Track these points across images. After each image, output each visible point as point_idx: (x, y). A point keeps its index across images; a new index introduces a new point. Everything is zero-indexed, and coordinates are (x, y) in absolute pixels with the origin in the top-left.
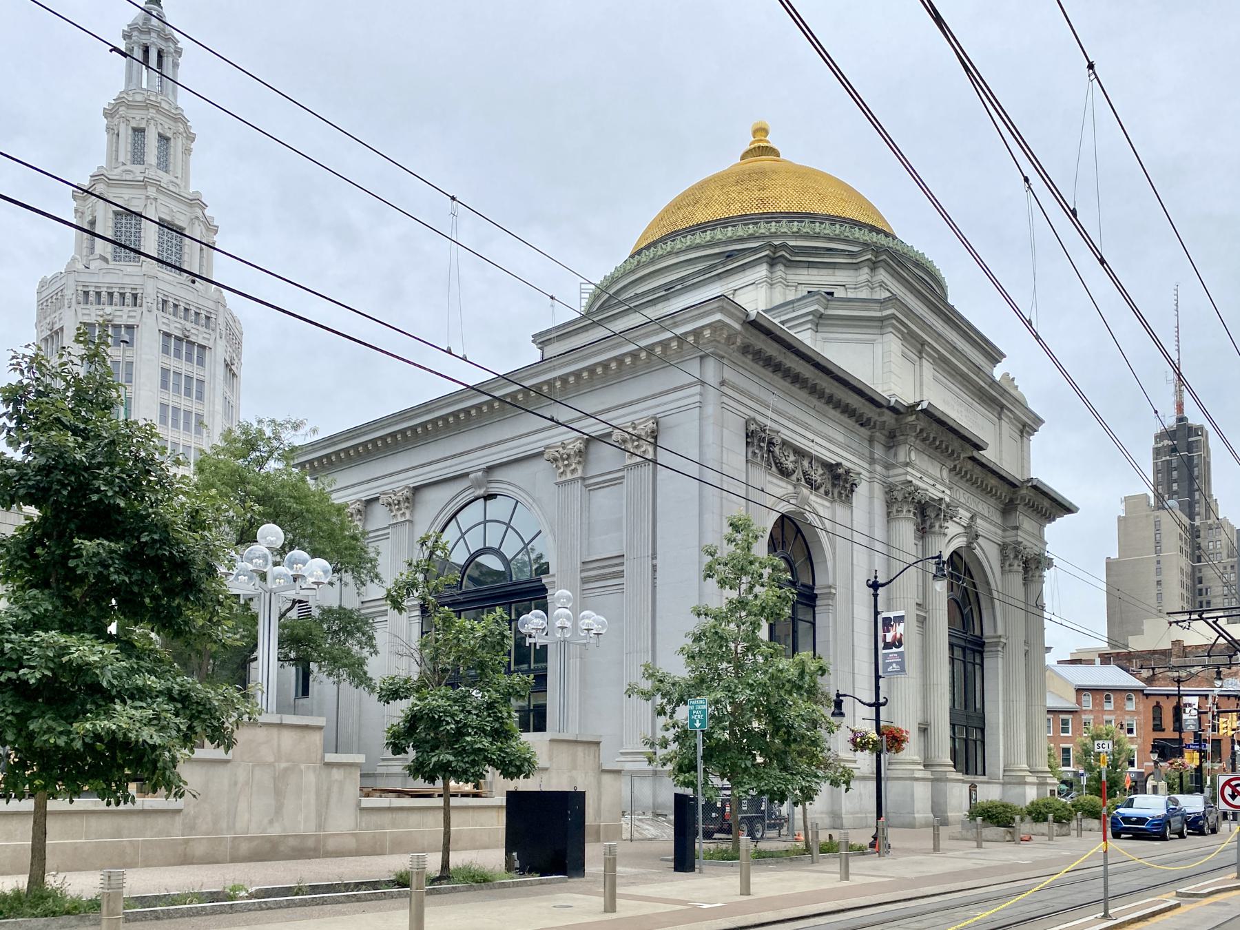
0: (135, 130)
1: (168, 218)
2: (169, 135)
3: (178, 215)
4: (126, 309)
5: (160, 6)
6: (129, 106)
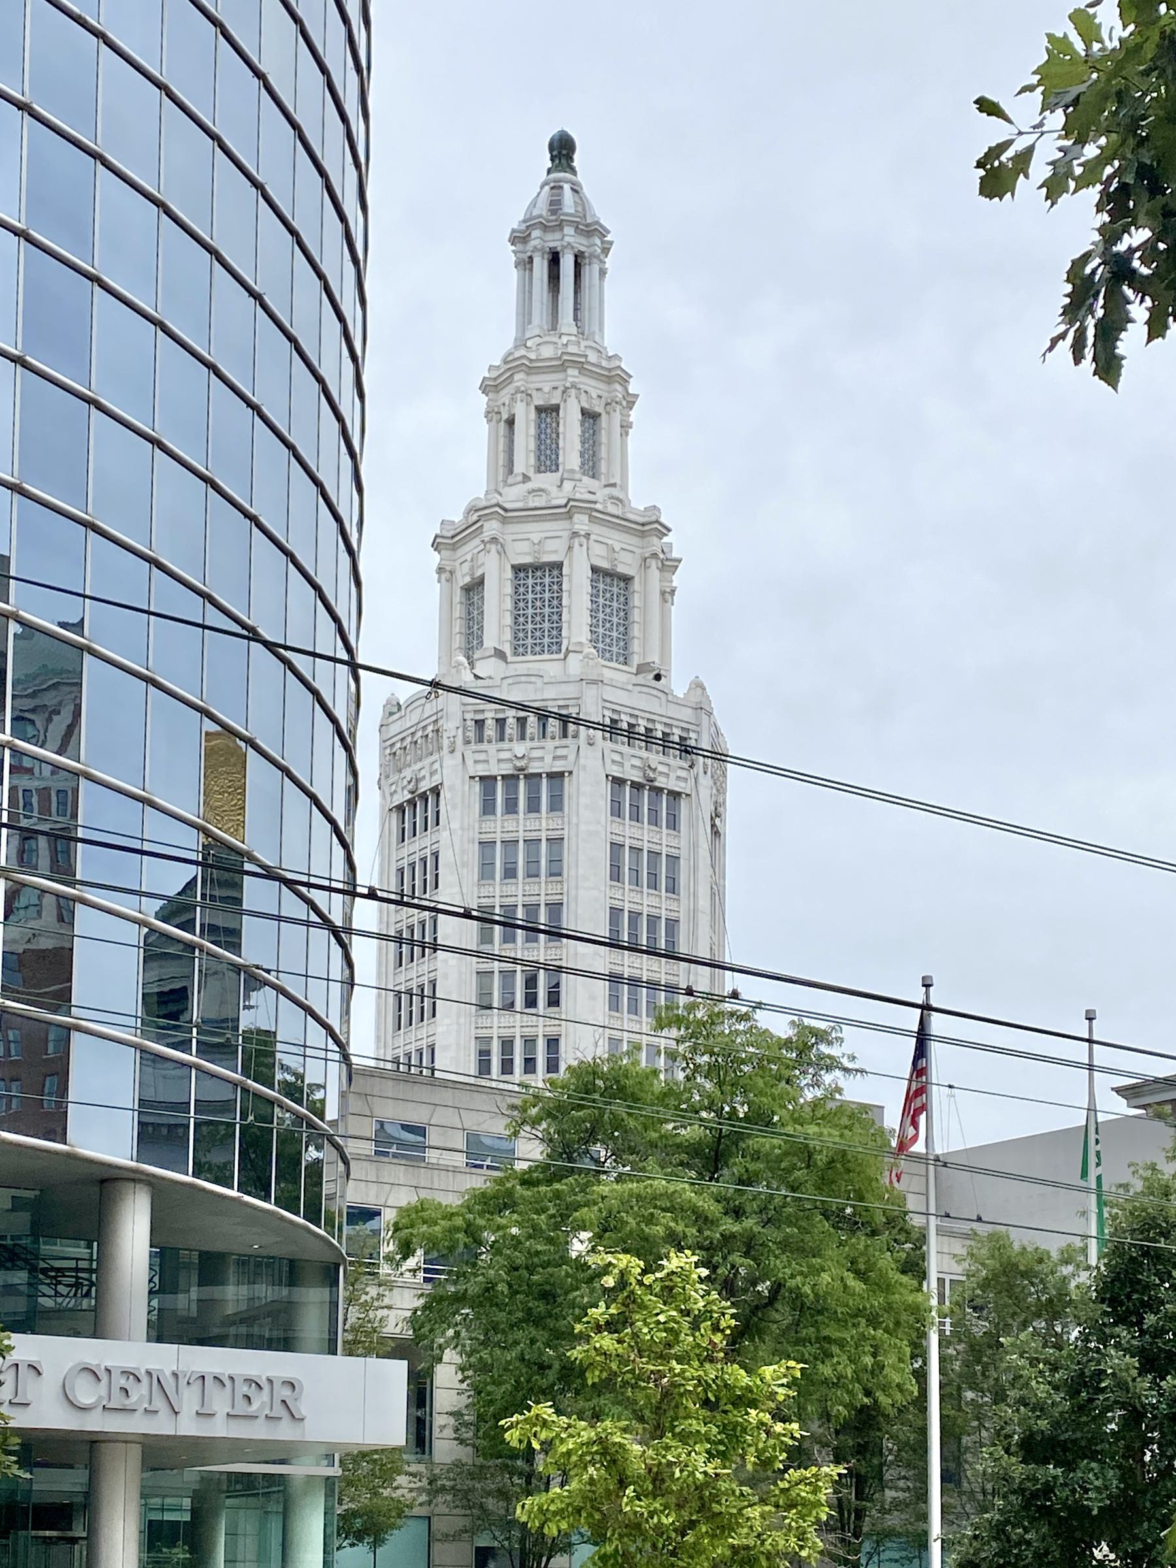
0: (540, 410)
1: (605, 564)
4: (549, 744)
5: (573, 171)
6: (531, 369)
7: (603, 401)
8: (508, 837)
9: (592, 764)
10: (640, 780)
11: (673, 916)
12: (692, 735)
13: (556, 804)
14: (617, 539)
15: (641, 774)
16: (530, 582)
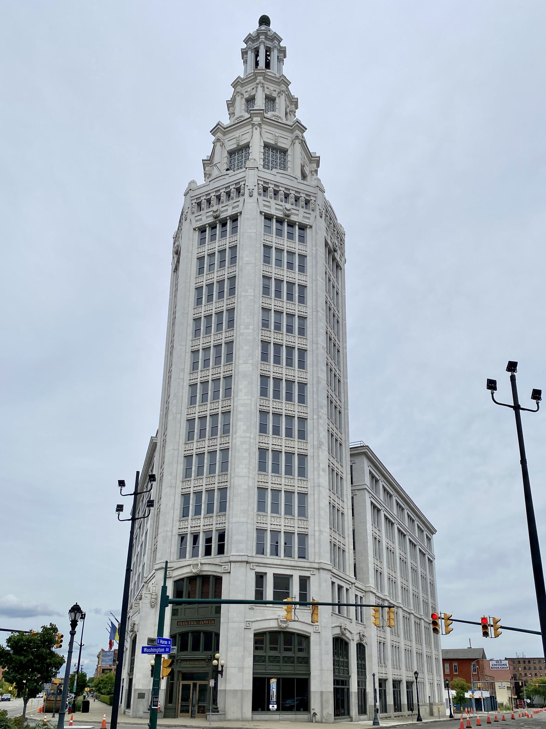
1: (272, 142)
2: (275, 95)
6: (243, 85)
7: (277, 92)
8: (210, 252)
10: (282, 216)
12: (312, 198)
13: (235, 230)
14: (278, 132)
15: (282, 213)
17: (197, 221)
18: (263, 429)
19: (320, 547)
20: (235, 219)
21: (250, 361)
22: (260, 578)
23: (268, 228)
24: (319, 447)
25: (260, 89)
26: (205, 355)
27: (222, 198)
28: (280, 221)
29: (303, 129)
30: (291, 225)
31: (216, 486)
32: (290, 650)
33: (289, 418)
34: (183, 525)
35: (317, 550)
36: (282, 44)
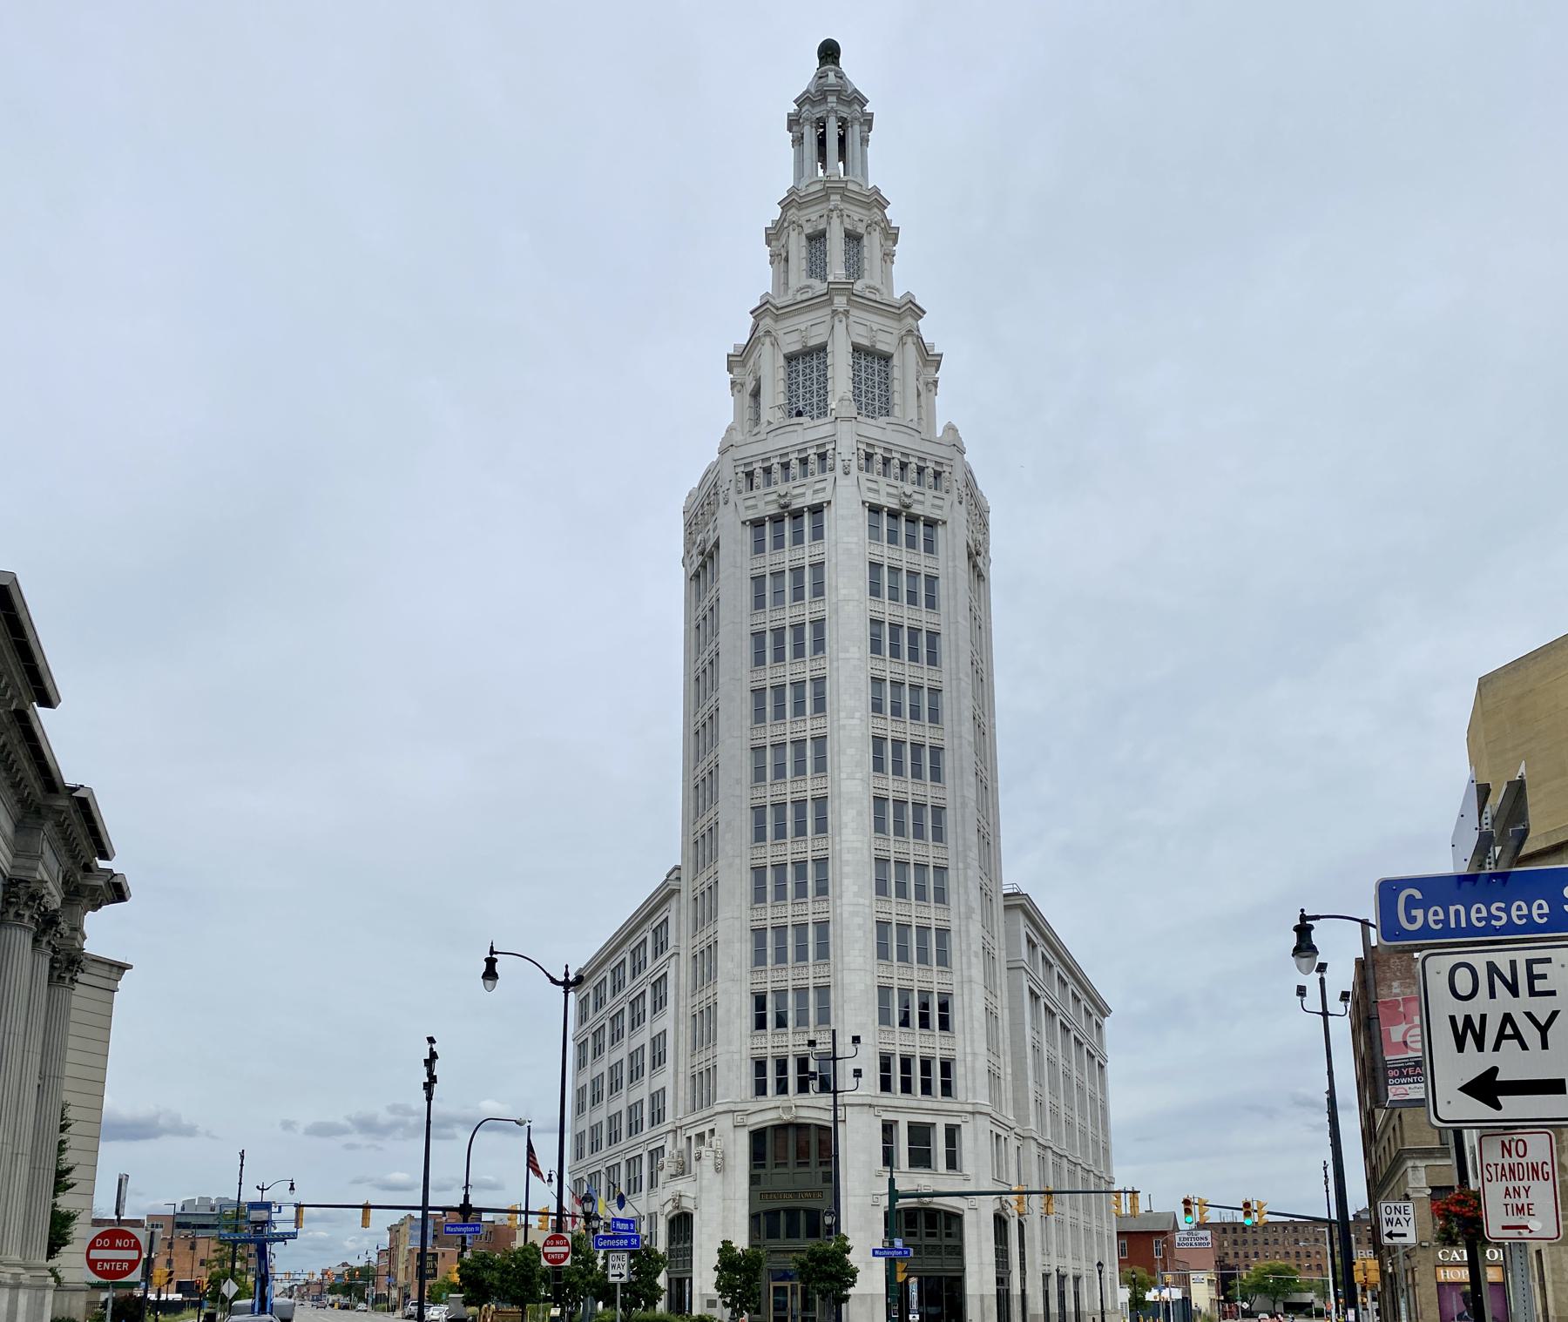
0: (810, 238)
1: (865, 342)
2: (861, 229)
3: (881, 336)
6: (800, 206)
8: (776, 568)
9: (847, 499)
11: (933, 628)
13: (818, 534)
14: (876, 321)
16: (801, 367)
17: (747, 508)
18: (881, 888)
19: (974, 1080)
20: (817, 510)
21: (858, 776)
22: (888, 1128)
23: (874, 528)
24: (968, 917)
25: (835, 221)
26: (776, 757)
27: (792, 471)
28: (894, 515)
29: (918, 312)
30: (913, 519)
31: (811, 983)
32: (934, 1235)
33: (921, 867)
34: (758, 1042)
35: (970, 1084)
36: (868, 109)
